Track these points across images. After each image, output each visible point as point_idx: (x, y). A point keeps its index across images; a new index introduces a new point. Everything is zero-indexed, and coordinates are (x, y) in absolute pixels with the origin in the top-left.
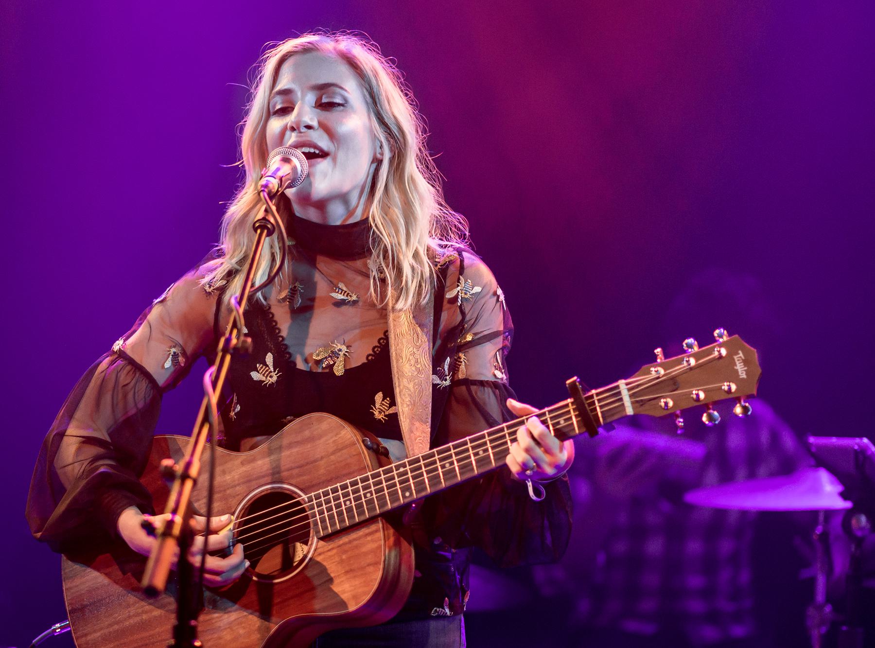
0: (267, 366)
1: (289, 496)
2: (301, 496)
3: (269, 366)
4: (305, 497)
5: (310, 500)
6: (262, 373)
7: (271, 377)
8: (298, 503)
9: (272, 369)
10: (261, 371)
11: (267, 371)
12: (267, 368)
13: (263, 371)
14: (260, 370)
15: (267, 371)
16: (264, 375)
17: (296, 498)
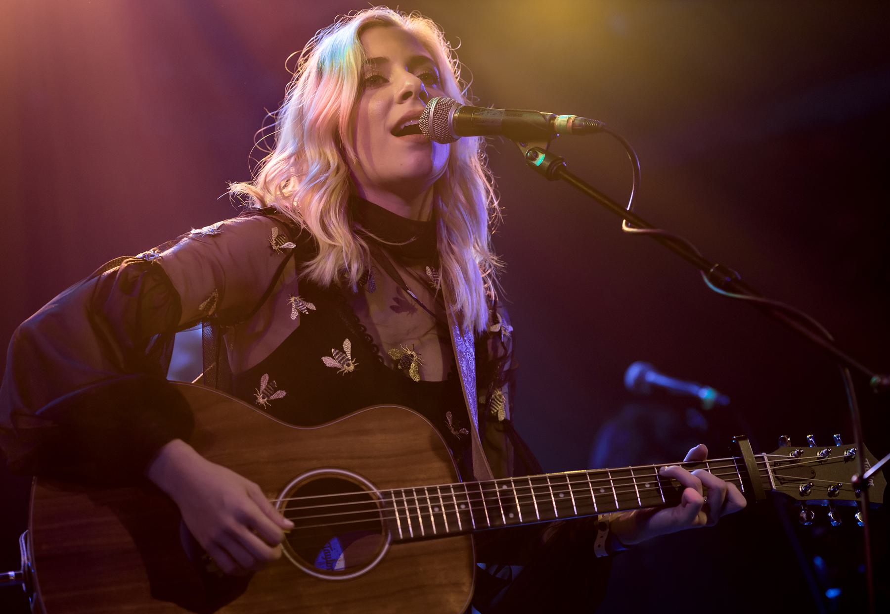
0: (344, 352)
1: (355, 486)
2: (370, 489)
3: (347, 353)
4: (378, 492)
5: (387, 495)
6: (337, 359)
7: (348, 365)
8: (367, 497)
9: (349, 357)
10: (337, 357)
11: (344, 357)
12: (345, 355)
13: (339, 357)
14: (336, 355)
15: (344, 357)
16: (339, 362)
17: (363, 490)
